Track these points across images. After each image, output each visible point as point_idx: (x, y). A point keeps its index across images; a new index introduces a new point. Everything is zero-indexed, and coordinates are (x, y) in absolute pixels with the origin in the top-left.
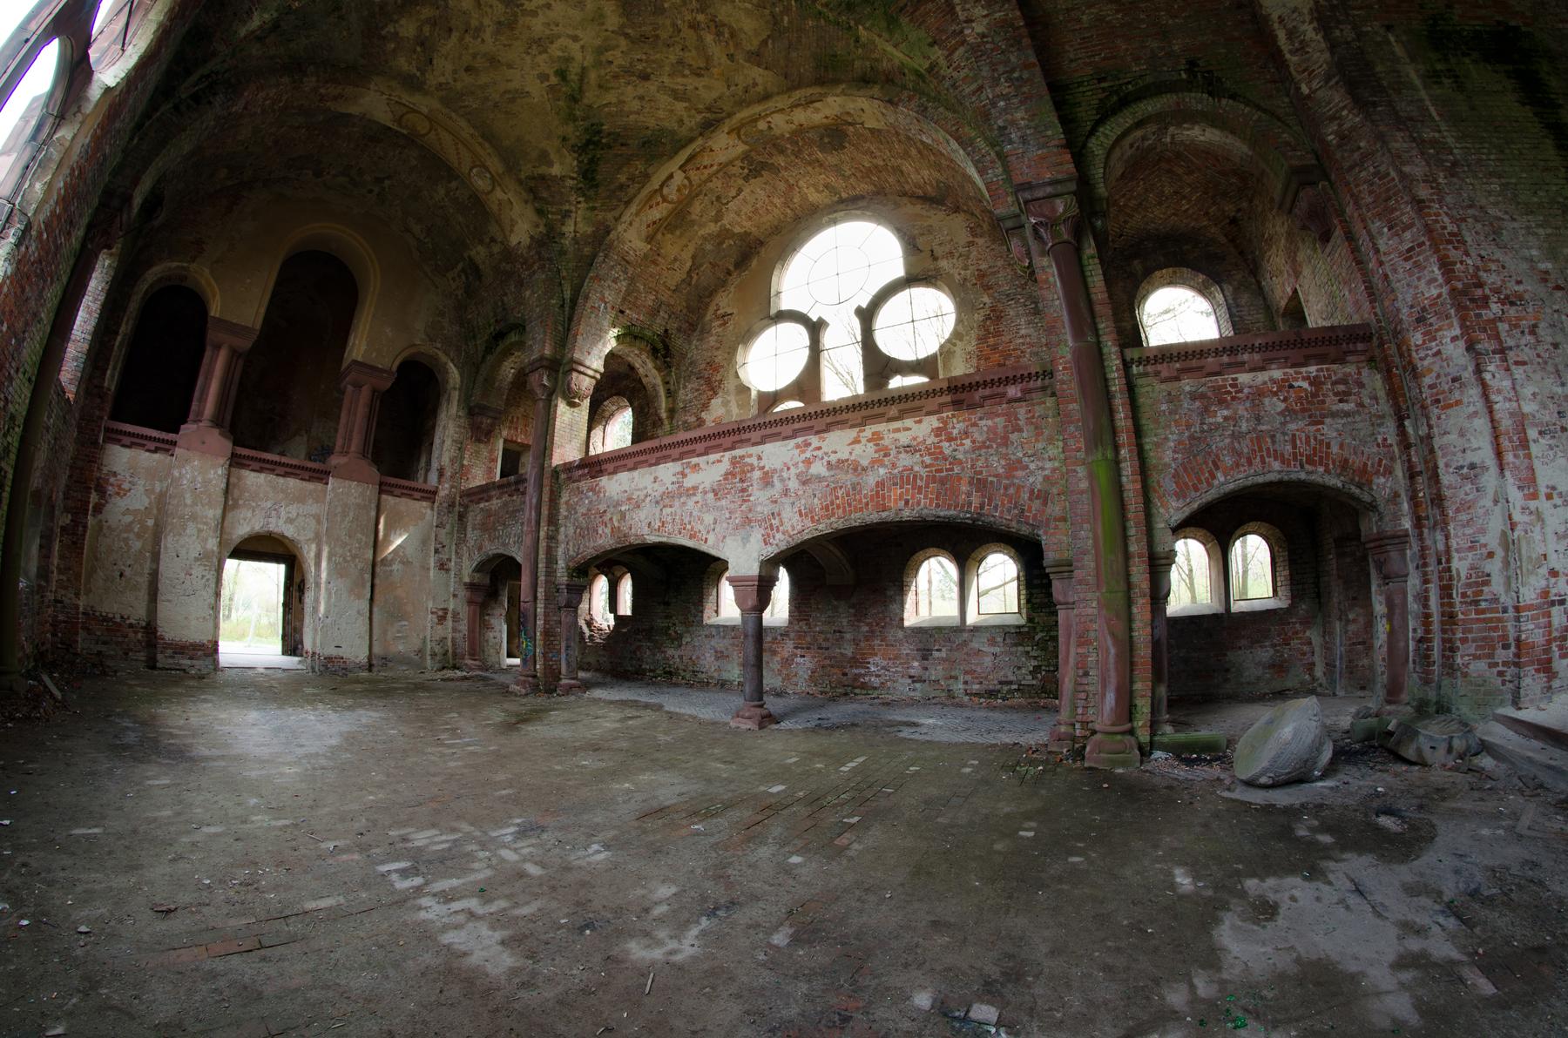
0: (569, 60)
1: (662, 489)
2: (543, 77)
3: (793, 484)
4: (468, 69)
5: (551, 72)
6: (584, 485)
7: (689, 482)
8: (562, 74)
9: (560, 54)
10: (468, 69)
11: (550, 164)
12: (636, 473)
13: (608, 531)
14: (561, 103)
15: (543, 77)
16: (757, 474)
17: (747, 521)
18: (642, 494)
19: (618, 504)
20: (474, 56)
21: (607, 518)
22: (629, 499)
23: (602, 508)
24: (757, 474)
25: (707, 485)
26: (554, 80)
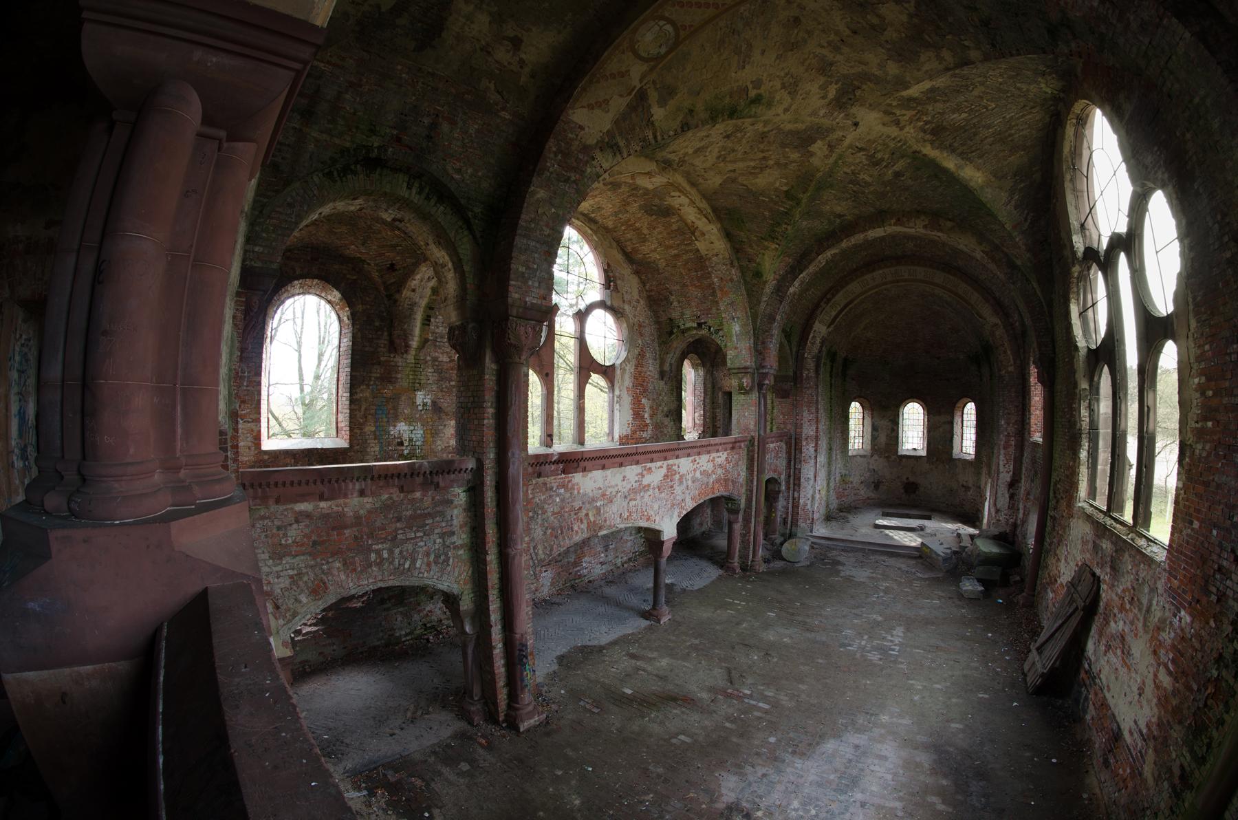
0: (770, 105)
1: (629, 486)
2: (757, 84)
3: (690, 483)
4: (797, 20)
5: (762, 91)
6: (552, 481)
7: (645, 481)
8: (758, 100)
9: (778, 98)
10: (797, 20)
11: (662, 103)
12: (609, 472)
13: (584, 526)
14: (727, 100)
15: (757, 84)
16: (677, 477)
17: (673, 505)
18: (614, 490)
19: (593, 500)
20: (808, 32)
21: (582, 515)
22: (603, 495)
23: (577, 505)
24: (677, 477)
25: (655, 484)
26: (753, 93)
